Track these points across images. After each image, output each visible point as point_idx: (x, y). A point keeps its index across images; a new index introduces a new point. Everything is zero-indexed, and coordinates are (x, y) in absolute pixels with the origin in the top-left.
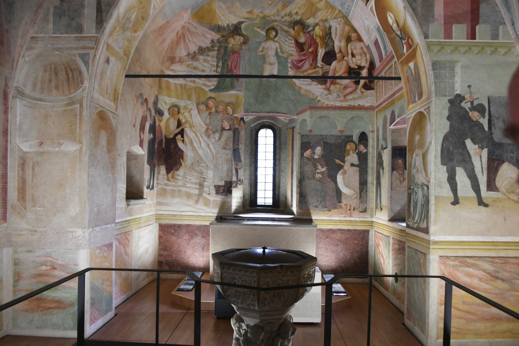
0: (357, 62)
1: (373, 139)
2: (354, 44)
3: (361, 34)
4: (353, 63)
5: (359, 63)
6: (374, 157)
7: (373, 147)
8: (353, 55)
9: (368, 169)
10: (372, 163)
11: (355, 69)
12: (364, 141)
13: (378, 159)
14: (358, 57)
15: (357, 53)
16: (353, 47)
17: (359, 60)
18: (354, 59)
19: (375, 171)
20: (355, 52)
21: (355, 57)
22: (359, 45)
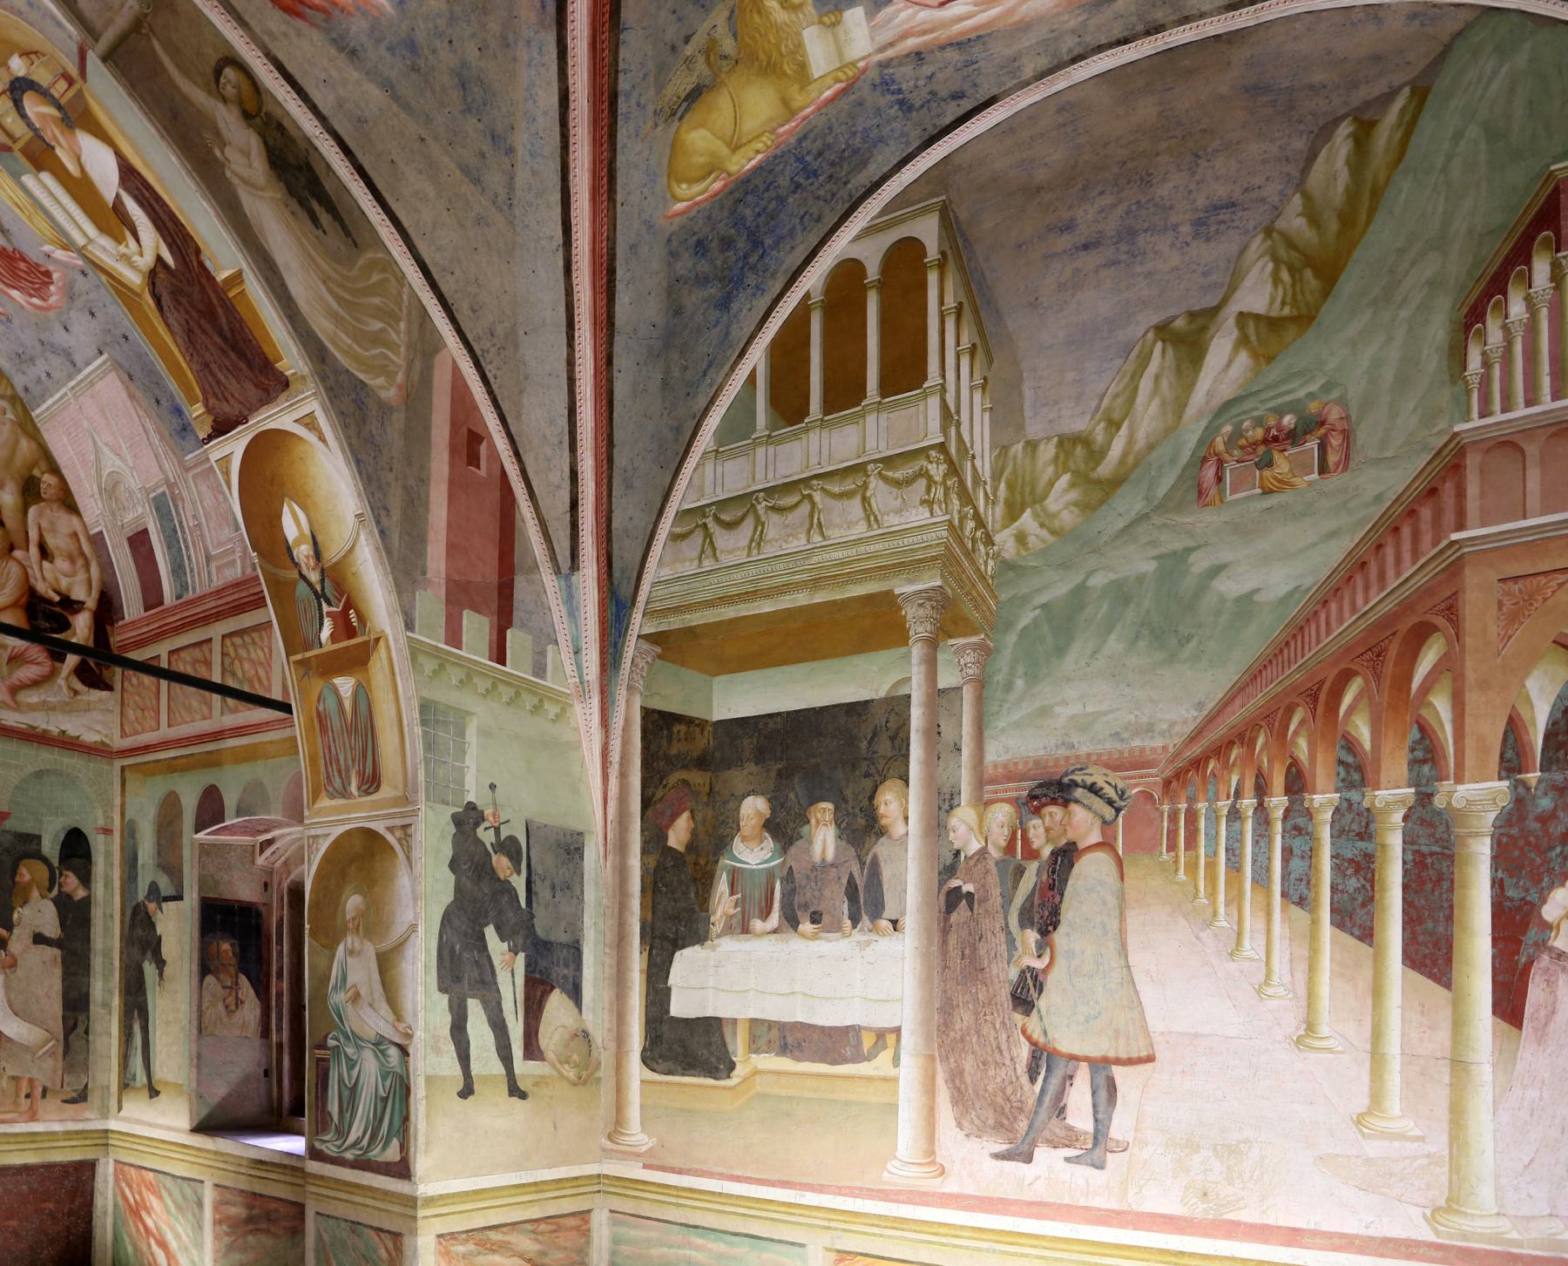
0: (57, 580)
1: (108, 855)
2: (48, 511)
3: (73, 488)
4: (44, 579)
5: (64, 583)
6: (112, 916)
7: (108, 883)
8: (45, 553)
9: (92, 956)
10: (107, 935)
11: (49, 602)
12: (76, 861)
13: (132, 926)
14: (62, 564)
15: (57, 548)
16: (44, 524)
17: (66, 576)
18: (46, 564)
19: (117, 963)
20: (51, 542)
21: (51, 562)
22: (66, 522)
